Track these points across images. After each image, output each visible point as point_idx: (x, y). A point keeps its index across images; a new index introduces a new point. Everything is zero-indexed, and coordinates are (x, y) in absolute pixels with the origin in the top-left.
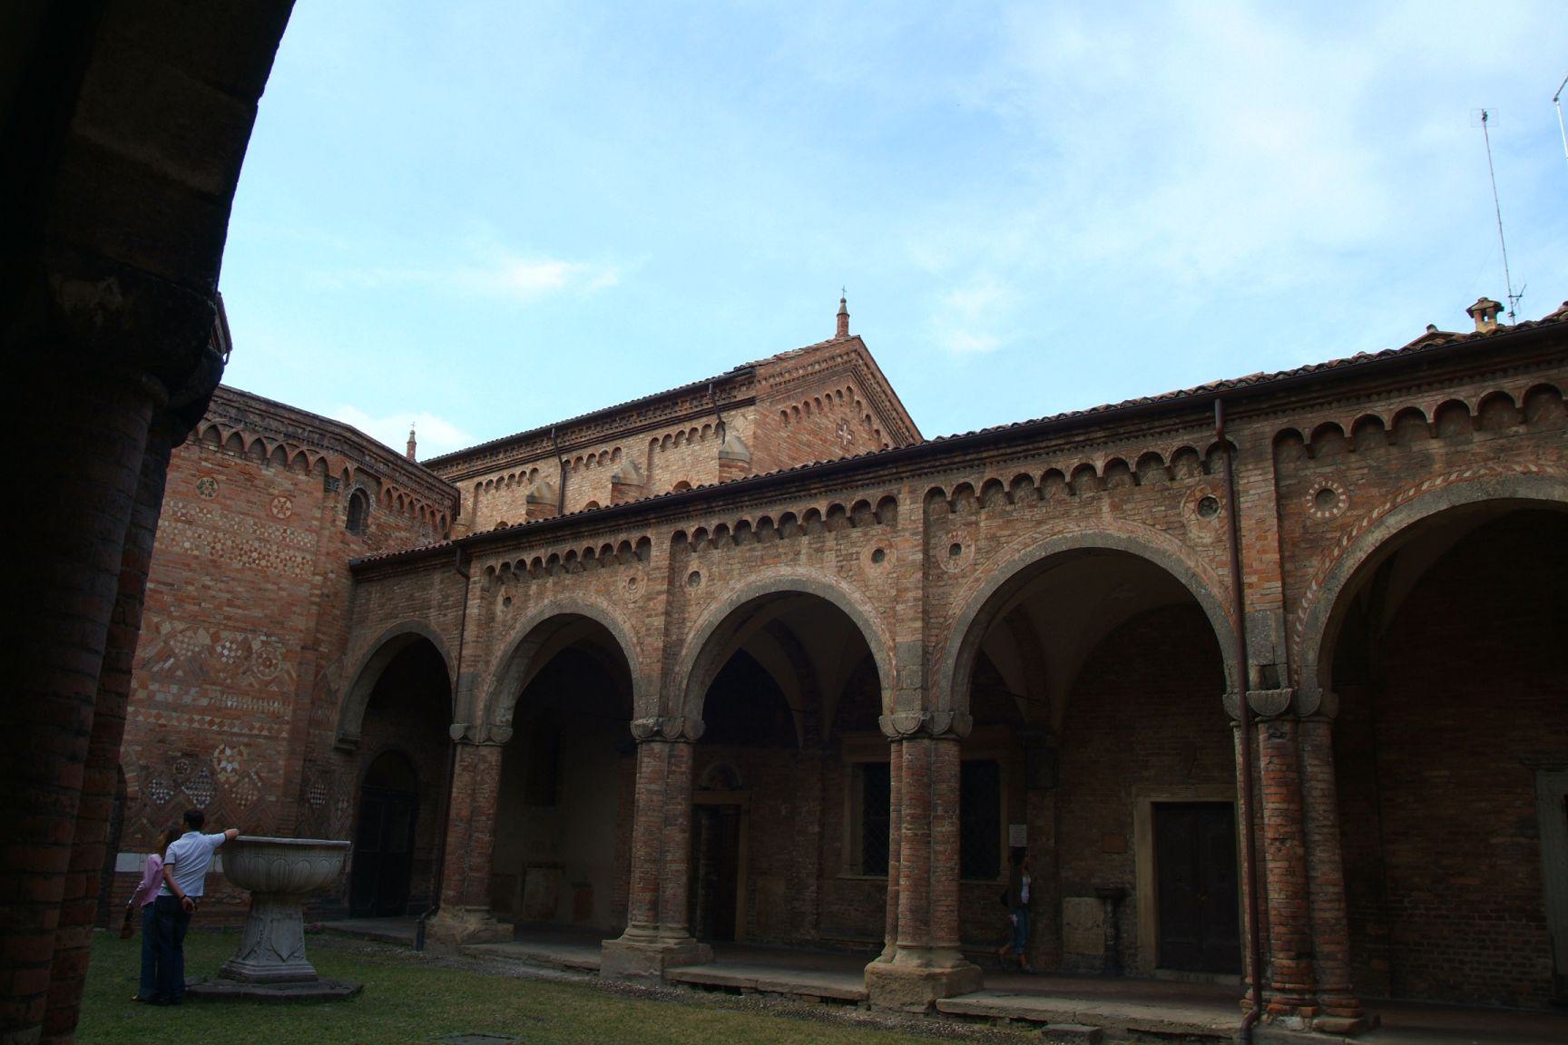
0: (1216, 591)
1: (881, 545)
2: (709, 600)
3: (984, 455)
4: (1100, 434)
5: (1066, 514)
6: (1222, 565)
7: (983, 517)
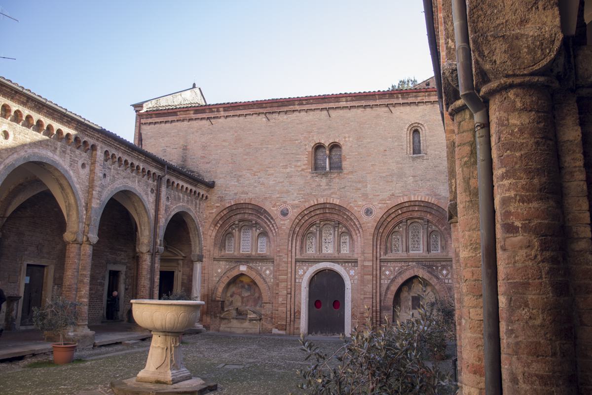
0: (152, 216)
1: (86, 162)
2: (13, 151)
3: (122, 148)
4: (144, 159)
5: (129, 178)
6: (153, 209)
7: (112, 168)
